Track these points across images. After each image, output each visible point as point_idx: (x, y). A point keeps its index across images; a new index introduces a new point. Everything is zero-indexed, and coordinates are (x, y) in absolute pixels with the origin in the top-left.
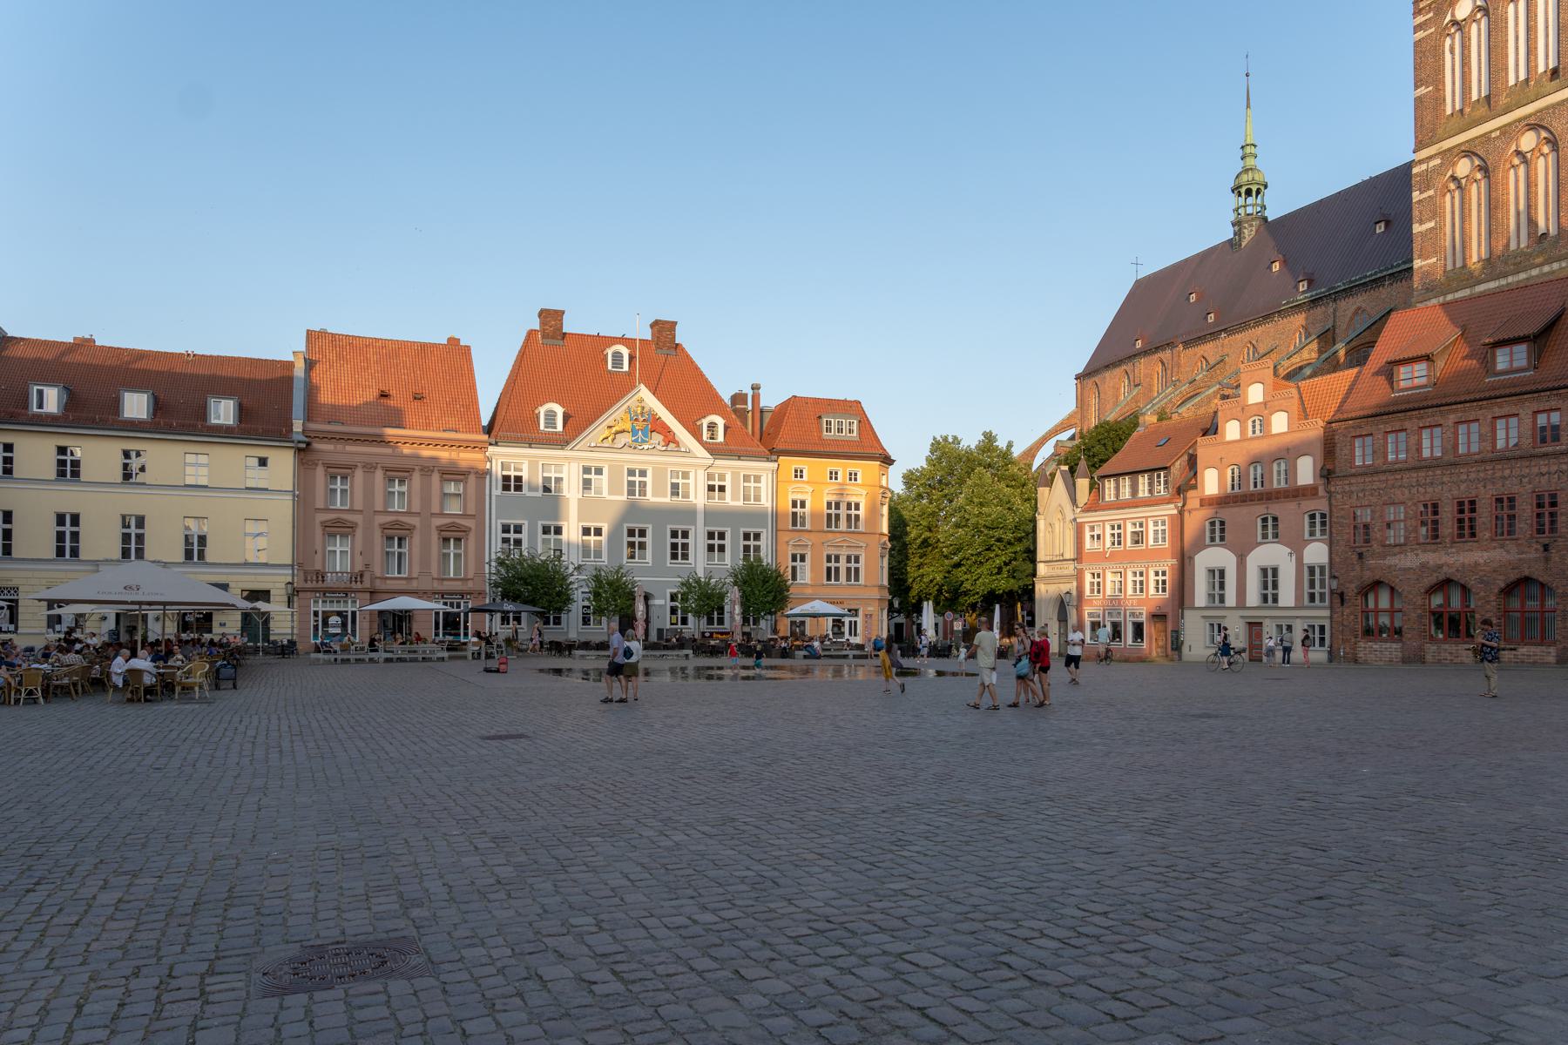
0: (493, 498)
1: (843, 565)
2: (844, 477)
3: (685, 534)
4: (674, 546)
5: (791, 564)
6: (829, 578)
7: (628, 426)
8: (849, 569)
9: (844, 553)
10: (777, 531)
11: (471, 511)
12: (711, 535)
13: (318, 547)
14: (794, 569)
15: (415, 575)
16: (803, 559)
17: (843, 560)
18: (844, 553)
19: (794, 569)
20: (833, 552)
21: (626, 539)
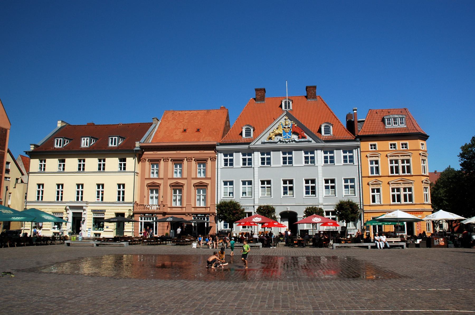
0: (219, 169)
1: (402, 193)
2: (399, 147)
3: (313, 181)
4: (307, 188)
5: (371, 194)
6: (394, 201)
7: (280, 131)
8: (405, 196)
9: (402, 187)
10: (362, 177)
11: (209, 175)
12: (327, 181)
13: (146, 194)
14: (374, 197)
15: (184, 206)
16: (378, 190)
17: (402, 190)
18: (402, 187)
19: (374, 197)
20: (395, 186)
21: (282, 185)
